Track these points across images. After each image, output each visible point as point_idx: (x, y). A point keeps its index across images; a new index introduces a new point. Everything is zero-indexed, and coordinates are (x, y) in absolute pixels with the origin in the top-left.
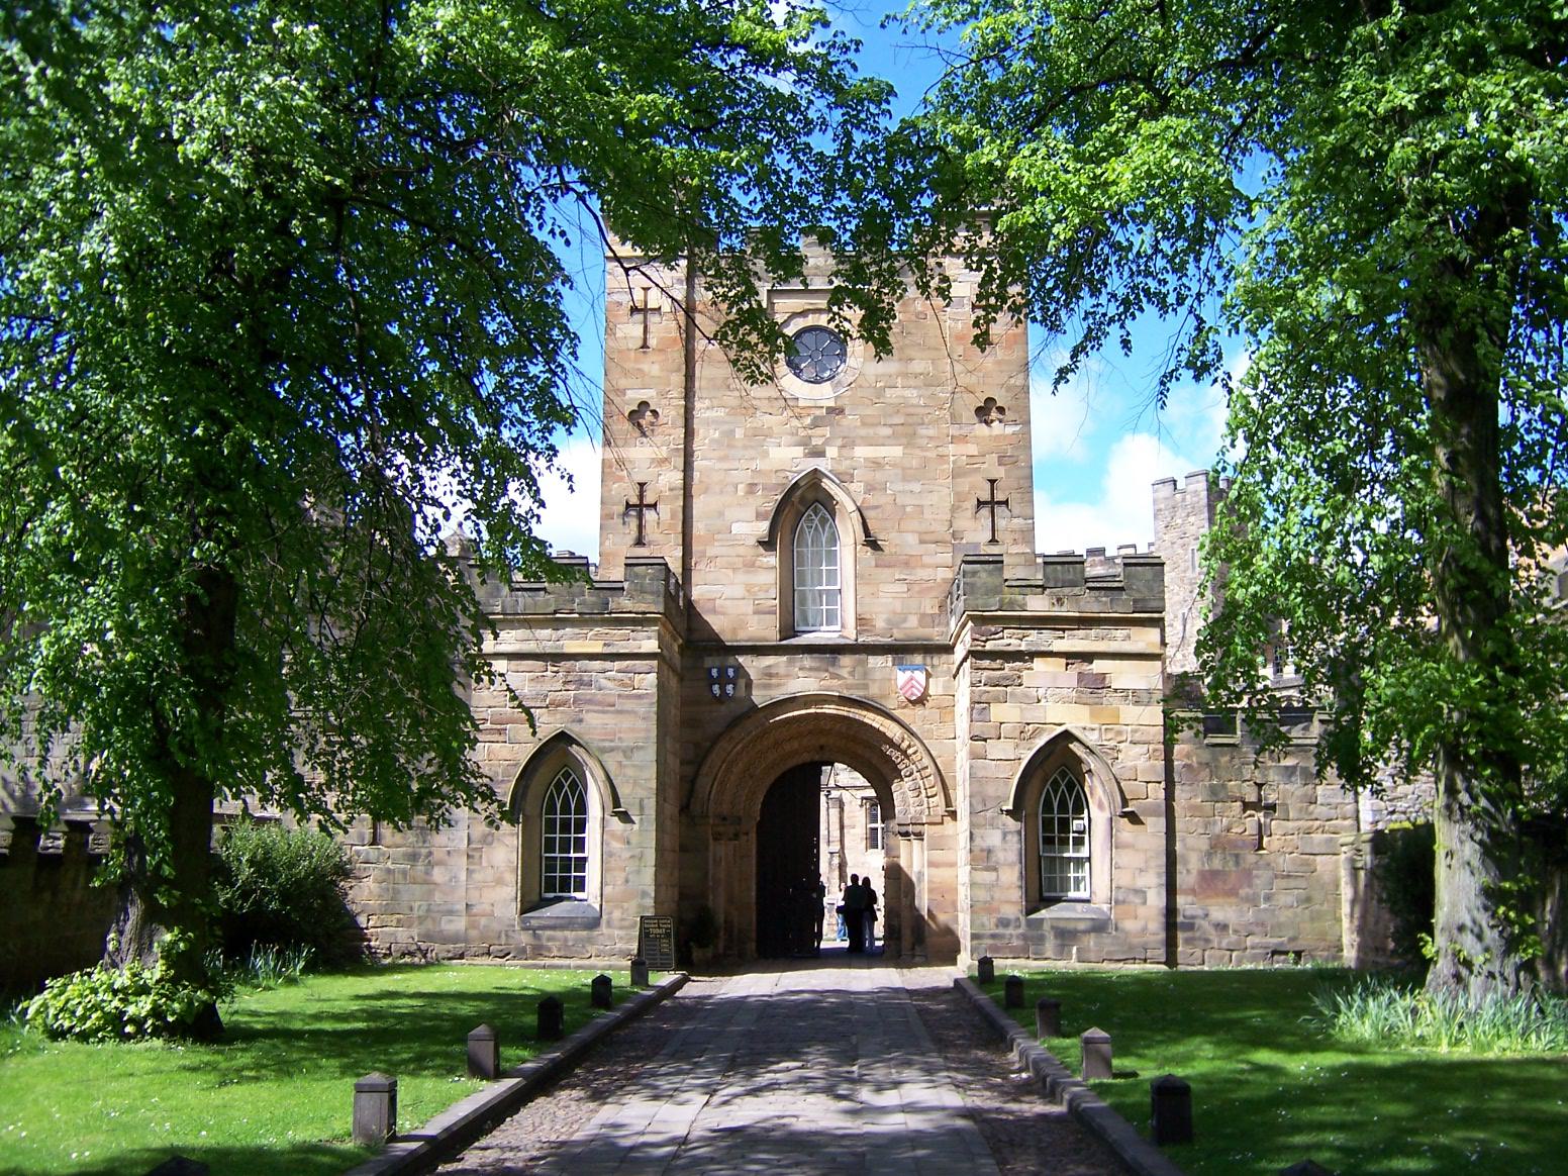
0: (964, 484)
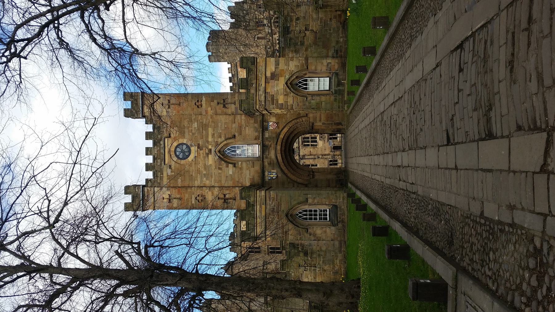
0: (219, 111)
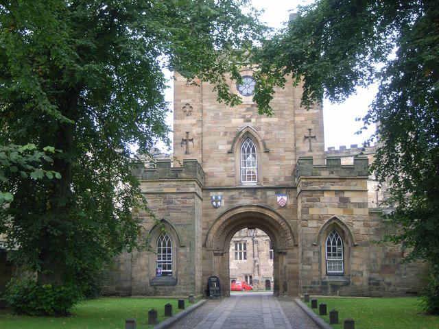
0: (299, 131)
